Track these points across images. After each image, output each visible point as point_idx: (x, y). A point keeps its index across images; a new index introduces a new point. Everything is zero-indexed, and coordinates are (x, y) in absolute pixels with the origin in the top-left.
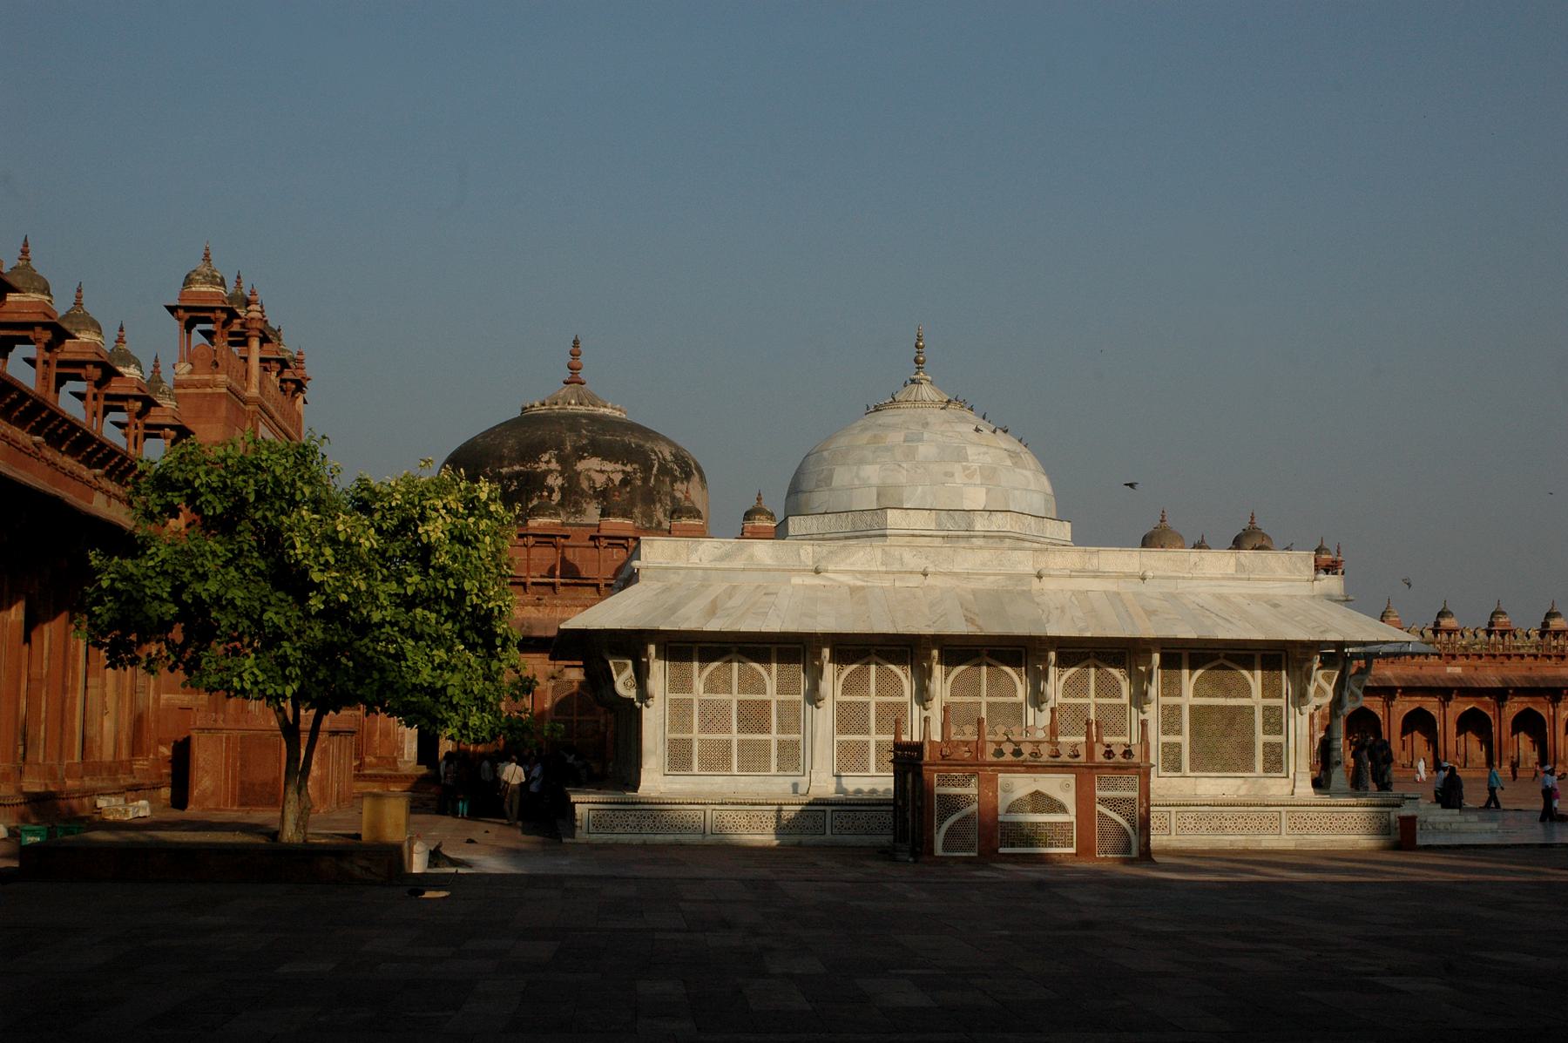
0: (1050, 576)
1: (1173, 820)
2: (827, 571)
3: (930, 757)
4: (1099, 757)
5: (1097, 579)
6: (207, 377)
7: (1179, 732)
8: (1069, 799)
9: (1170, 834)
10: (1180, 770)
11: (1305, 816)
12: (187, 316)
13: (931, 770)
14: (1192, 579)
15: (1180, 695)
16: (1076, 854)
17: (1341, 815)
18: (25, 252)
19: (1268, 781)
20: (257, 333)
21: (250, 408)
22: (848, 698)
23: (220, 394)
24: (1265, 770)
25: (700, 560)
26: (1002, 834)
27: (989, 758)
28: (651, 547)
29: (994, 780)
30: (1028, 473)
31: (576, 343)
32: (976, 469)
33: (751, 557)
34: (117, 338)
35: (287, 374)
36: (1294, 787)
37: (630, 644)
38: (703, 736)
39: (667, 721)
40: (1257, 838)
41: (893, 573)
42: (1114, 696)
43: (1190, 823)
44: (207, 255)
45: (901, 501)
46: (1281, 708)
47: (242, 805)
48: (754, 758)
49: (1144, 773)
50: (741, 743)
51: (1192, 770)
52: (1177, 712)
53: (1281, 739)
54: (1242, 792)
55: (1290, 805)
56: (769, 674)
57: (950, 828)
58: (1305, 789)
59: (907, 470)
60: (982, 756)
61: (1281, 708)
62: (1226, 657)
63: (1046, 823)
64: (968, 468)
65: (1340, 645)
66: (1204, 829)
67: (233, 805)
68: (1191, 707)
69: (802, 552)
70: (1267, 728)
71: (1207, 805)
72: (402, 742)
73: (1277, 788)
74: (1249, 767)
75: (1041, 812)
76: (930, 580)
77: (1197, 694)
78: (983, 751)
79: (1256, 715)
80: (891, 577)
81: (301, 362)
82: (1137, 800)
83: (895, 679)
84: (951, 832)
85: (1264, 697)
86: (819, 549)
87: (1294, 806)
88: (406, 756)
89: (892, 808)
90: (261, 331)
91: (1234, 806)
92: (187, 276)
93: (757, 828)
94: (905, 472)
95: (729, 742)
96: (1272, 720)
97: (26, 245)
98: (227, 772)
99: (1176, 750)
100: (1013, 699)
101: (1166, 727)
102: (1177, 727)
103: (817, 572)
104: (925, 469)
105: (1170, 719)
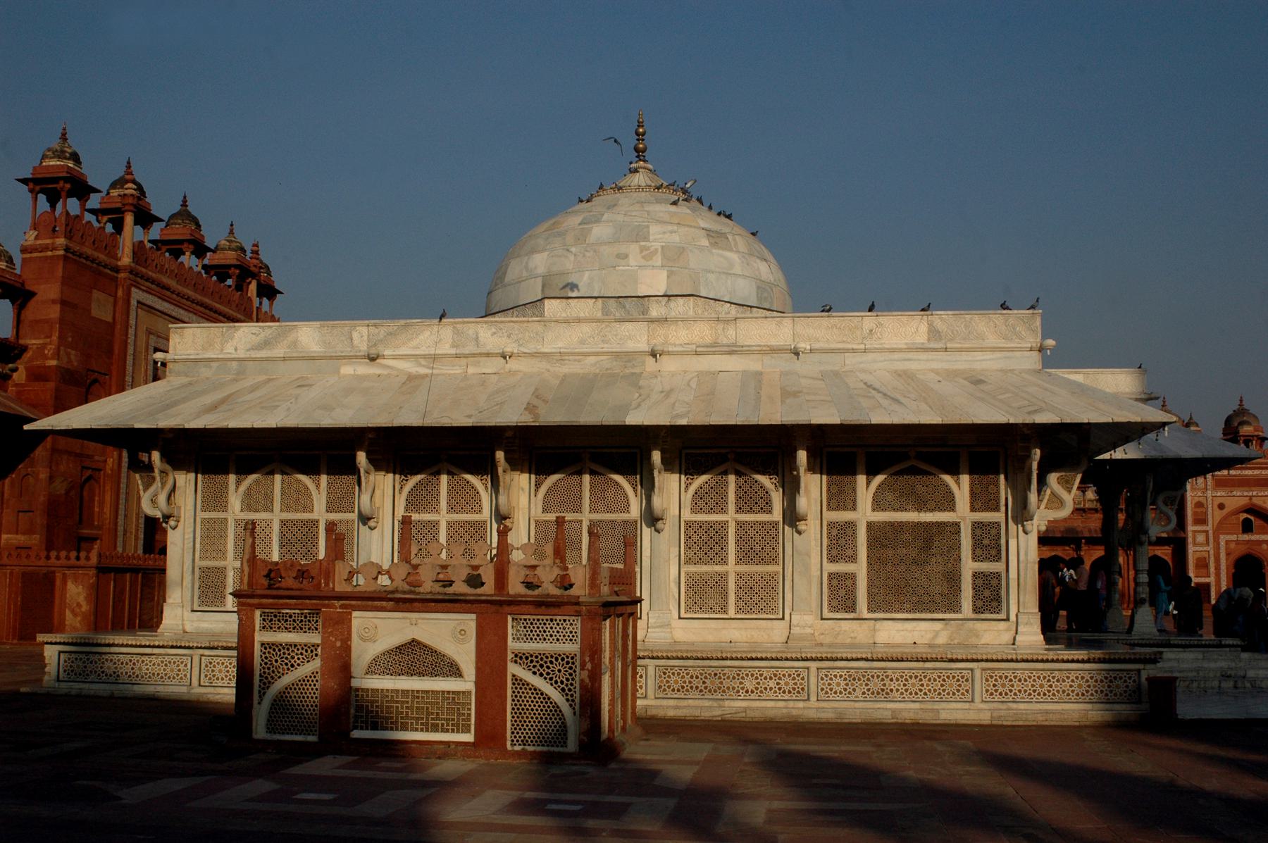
0: (669, 353)
1: (813, 680)
2: (383, 357)
5: (734, 357)
6: (48, 241)
7: (853, 559)
8: (465, 654)
9: (808, 699)
10: (854, 611)
11: (1010, 674)
13: (250, 605)
14: (865, 351)
16: (473, 744)
17: (1065, 674)
19: (979, 626)
20: (132, 208)
21: (122, 275)
23: (58, 256)
24: (976, 610)
25: (236, 350)
27: (340, 587)
29: (345, 622)
30: (734, 257)
32: (656, 250)
33: (295, 344)
36: (1016, 633)
39: (198, 546)
40: (936, 706)
41: (466, 356)
42: (762, 511)
43: (838, 685)
44: (64, 134)
46: (998, 524)
47: (21, 638)
52: (849, 532)
54: (942, 639)
55: (987, 661)
56: (318, 486)
58: (1031, 636)
59: (575, 255)
60: (327, 584)
61: (998, 524)
63: (427, 692)
64: (647, 248)
66: (858, 692)
67: (13, 639)
68: (870, 526)
69: (355, 335)
70: (979, 552)
71: (862, 659)
74: (955, 607)
75: (421, 674)
76: (513, 365)
79: (963, 534)
80: (464, 361)
82: (578, 658)
83: (473, 493)
85: (973, 509)
86: (377, 331)
87: (992, 661)
90: (135, 206)
91: (902, 660)
93: (222, 679)
94: (572, 258)
96: (986, 542)
99: (849, 583)
100: (624, 516)
101: (834, 552)
102: (850, 552)
103: (373, 359)
104: (595, 251)
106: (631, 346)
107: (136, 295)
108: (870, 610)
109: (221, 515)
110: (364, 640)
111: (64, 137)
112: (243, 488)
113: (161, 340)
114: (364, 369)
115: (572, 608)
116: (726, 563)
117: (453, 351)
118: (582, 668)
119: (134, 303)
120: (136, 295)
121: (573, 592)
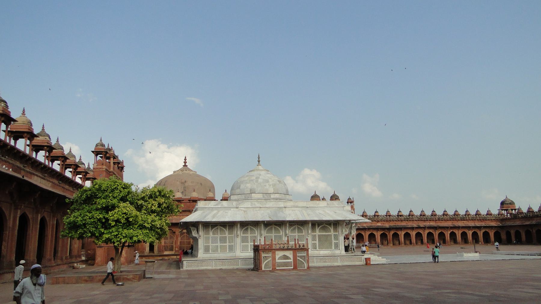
1: (315, 260)
2: (239, 207)
3: (261, 248)
4: (298, 247)
7: (316, 241)
8: (291, 256)
10: (316, 249)
12: (96, 153)
14: (318, 207)
18: (58, 140)
21: (111, 173)
22: (244, 235)
24: (335, 248)
26: (277, 265)
27: (274, 248)
31: (185, 157)
33: (222, 205)
34: (80, 159)
35: (120, 166)
37: (195, 225)
38: (212, 244)
40: (333, 263)
44: (101, 139)
45: (255, 192)
48: (223, 249)
49: (307, 250)
50: (220, 246)
53: (338, 241)
54: (330, 253)
57: (266, 263)
58: (343, 252)
61: (337, 235)
62: (326, 224)
64: (269, 184)
65: (350, 221)
68: (318, 235)
72: (146, 247)
73: (337, 252)
78: (272, 247)
81: (123, 162)
85: (334, 232)
88: (146, 251)
89: (253, 259)
92: (96, 144)
94: (256, 185)
95: (217, 246)
97: (58, 138)
98: (104, 256)
102: (315, 240)
105: (314, 239)
106: (280, 206)
109: (209, 236)
110: (278, 255)
111: (101, 140)
114: (235, 209)
115: (305, 250)
117: (251, 206)
118: (307, 257)
121: (304, 247)
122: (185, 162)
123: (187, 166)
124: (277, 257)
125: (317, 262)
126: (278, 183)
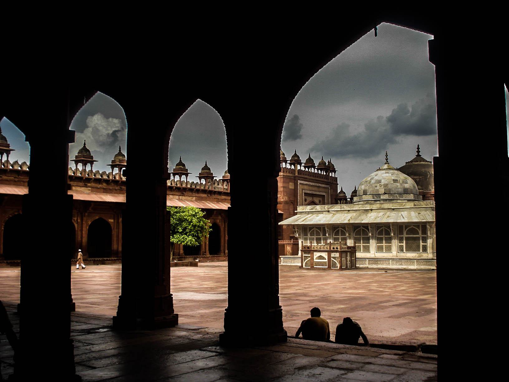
4: (332, 249)
7: (403, 243)
8: (326, 257)
15: (403, 235)
19: (423, 254)
26: (315, 264)
27: (313, 249)
28: (299, 208)
31: (418, 146)
51: (406, 251)
57: (306, 262)
62: (413, 226)
64: (380, 185)
68: (405, 237)
77: (407, 234)
80: (342, 211)
84: (306, 263)
107: (299, 182)
108: (406, 251)
109: (307, 237)
112: (310, 232)
113: (306, 191)
114: (327, 213)
116: (383, 243)
117: (340, 210)
119: (299, 184)
120: (299, 182)
122: (418, 152)
123: (421, 156)
124: (315, 257)
125: (392, 264)
126: (392, 182)
